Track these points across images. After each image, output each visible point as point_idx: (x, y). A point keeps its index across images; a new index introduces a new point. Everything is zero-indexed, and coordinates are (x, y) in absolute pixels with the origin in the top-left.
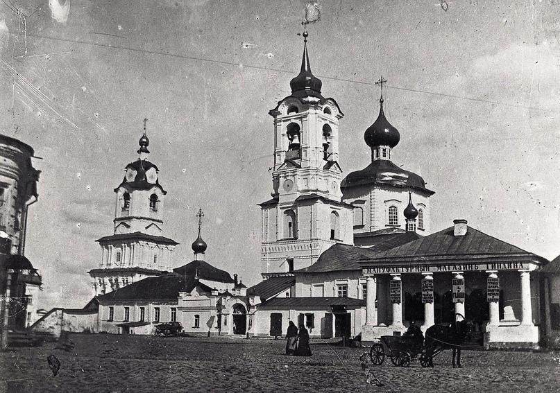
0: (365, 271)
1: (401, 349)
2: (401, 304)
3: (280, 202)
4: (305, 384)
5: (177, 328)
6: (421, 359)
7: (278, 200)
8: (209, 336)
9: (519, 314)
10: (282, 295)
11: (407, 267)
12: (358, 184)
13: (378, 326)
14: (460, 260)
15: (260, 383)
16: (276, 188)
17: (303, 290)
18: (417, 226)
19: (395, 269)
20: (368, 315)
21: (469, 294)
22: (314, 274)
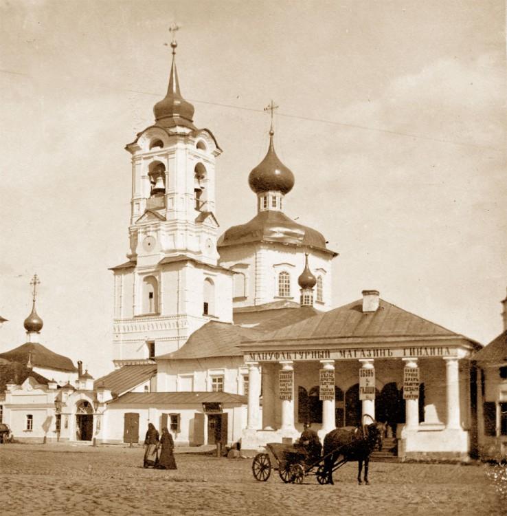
0: (247, 357)
1: (307, 459)
2: (292, 401)
3: (138, 266)
4: (169, 507)
5: (4, 432)
6: (318, 473)
7: (135, 262)
8: (45, 442)
9: (443, 416)
10: (140, 389)
11: (301, 352)
12: (239, 241)
13: (263, 430)
14: (370, 343)
15: (110, 504)
16: (133, 247)
17: (166, 382)
18: (315, 299)
19: (286, 355)
20: (251, 416)
21: (380, 389)
22: (181, 361)
